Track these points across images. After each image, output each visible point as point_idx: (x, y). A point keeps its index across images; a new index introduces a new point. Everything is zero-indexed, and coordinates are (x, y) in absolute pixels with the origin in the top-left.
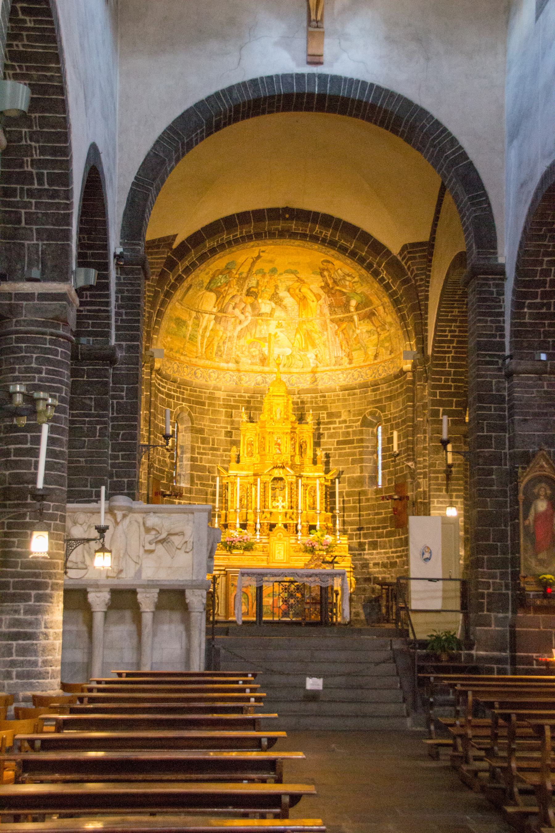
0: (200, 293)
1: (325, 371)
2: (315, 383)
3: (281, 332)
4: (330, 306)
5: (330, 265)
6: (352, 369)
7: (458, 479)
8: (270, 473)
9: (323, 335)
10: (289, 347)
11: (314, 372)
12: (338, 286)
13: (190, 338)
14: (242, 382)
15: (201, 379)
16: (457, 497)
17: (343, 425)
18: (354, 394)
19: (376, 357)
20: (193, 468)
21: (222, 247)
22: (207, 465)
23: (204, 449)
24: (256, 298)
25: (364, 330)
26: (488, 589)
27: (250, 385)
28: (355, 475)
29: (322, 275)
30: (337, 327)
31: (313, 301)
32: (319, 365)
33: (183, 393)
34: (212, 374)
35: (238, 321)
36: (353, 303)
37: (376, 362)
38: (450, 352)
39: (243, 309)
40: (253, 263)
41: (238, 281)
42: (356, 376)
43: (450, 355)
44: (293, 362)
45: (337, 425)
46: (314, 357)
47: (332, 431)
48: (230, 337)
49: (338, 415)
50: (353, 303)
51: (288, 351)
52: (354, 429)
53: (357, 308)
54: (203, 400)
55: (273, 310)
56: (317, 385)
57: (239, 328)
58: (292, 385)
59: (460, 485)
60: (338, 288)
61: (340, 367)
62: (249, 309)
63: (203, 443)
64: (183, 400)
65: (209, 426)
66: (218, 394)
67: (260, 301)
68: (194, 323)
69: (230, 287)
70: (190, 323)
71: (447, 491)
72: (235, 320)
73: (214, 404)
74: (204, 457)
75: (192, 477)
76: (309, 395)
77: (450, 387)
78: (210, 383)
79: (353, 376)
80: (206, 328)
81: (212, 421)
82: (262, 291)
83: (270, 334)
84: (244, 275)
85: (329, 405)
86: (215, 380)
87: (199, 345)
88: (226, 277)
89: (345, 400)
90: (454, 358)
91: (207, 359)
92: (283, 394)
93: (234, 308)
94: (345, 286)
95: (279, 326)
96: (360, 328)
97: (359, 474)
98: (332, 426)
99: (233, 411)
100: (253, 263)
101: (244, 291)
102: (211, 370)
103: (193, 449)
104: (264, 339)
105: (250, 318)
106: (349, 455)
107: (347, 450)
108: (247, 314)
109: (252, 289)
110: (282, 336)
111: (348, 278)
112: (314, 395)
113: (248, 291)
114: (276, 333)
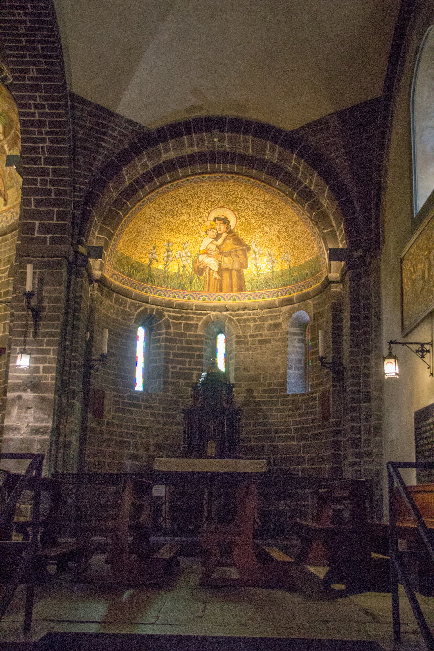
6: (5, 211)
7: (51, 318)
16: (49, 343)
18: (6, 240)
38: (43, 140)
42: (9, 218)
43: (45, 145)
59: (54, 327)
71: (35, 335)
77: (49, 192)
79: (7, 218)
90: (51, 150)
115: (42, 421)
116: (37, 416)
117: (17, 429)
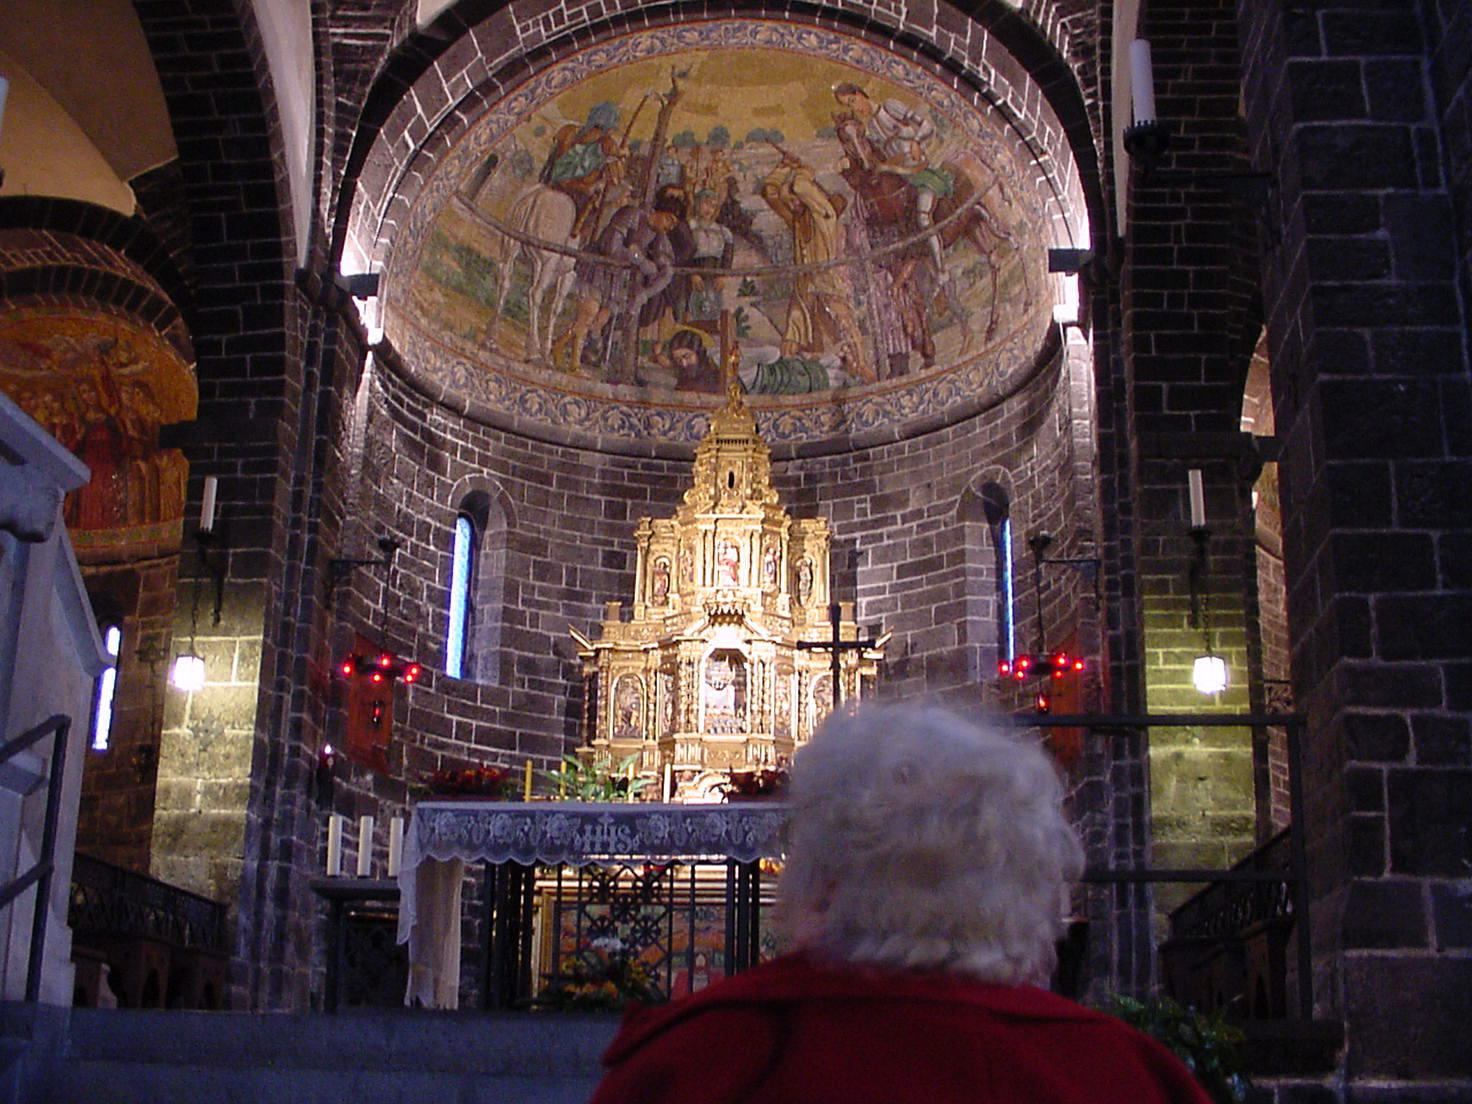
0: (528, 190)
1: (867, 394)
2: (842, 428)
3: (753, 305)
4: (871, 223)
5: (858, 97)
6: (930, 379)
8: (703, 636)
9: (859, 303)
10: (772, 343)
11: (838, 402)
12: (884, 161)
13: (507, 311)
14: (654, 431)
15: (539, 416)
17: (914, 524)
19: (990, 332)
20: (510, 637)
21: (562, 44)
22: (552, 635)
23: (543, 592)
24: (682, 217)
25: (960, 271)
26: (1399, 755)
27: (673, 439)
28: (945, 650)
29: (844, 140)
30: (890, 278)
31: (827, 216)
32: (852, 382)
33: (485, 445)
34: (572, 408)
35: (639, 278)
36: (926, 202)
37: (990, 345)
38: (1179, 214)
39: (651, 246)
40: (664, 114)
41: (629, 168)
43: (1181, 223)
44: (786, 379)
45: (899, 526)
46: (838, 362)
47: (886, 542)
48: (619, 316)
49: (901, 500)
50: (926, 202)
51: (774, 354)
52: (943, 528)
53: (937, 215)
54: (544, 470)
55: (729, 249)
56: (847, 431)
57: (643, 298)
58: (783, 436)
60: (885, 168)
61: (904, 379)
62: (666, 246)
63: (539, 577)
64: (484, 461)
65: (561, 535)
66: (586, 458)
67: (693, 224)
68: (516, 272)
69: (610, 183)
70: (506, 269)
72: (633, 275)
73: (577, 482)
74: (545, 612)
75: (505, 662)
76: (828, 458)
78: (564, 427)
79: (935, 394)
80: (552, 289)
81: (567, 523)
82: (697, 197)
83: (724, 313)
84: (645, 151)
85: (877, 478)
86: (581, 422)
87: (536, 332)
88: (595, 152)
89: (916, 460)
91: (558, 369)
92: (743, 437)
93: (626, 243)
94: (900, 162)
95: (747, 290)
96: (947, 267)
97: (956, 646)
98: (884, 530)
99: (629, 502)
100: (664, 114)
101: (650, 196)
102: (568, 399)
103: (511, 591)
104: (710, 327)
105: (671, 271)
106: (931, 597)
107: (926, 588)
108: (662, 260)
109: (671, 192)
110: (755, 316)
111: (907, 131)
112: (838, 457)
113: (660, 194)
114: (740, 310)
115: (1233, 805)
116: (1222, 795)
117: (1181, 824)
